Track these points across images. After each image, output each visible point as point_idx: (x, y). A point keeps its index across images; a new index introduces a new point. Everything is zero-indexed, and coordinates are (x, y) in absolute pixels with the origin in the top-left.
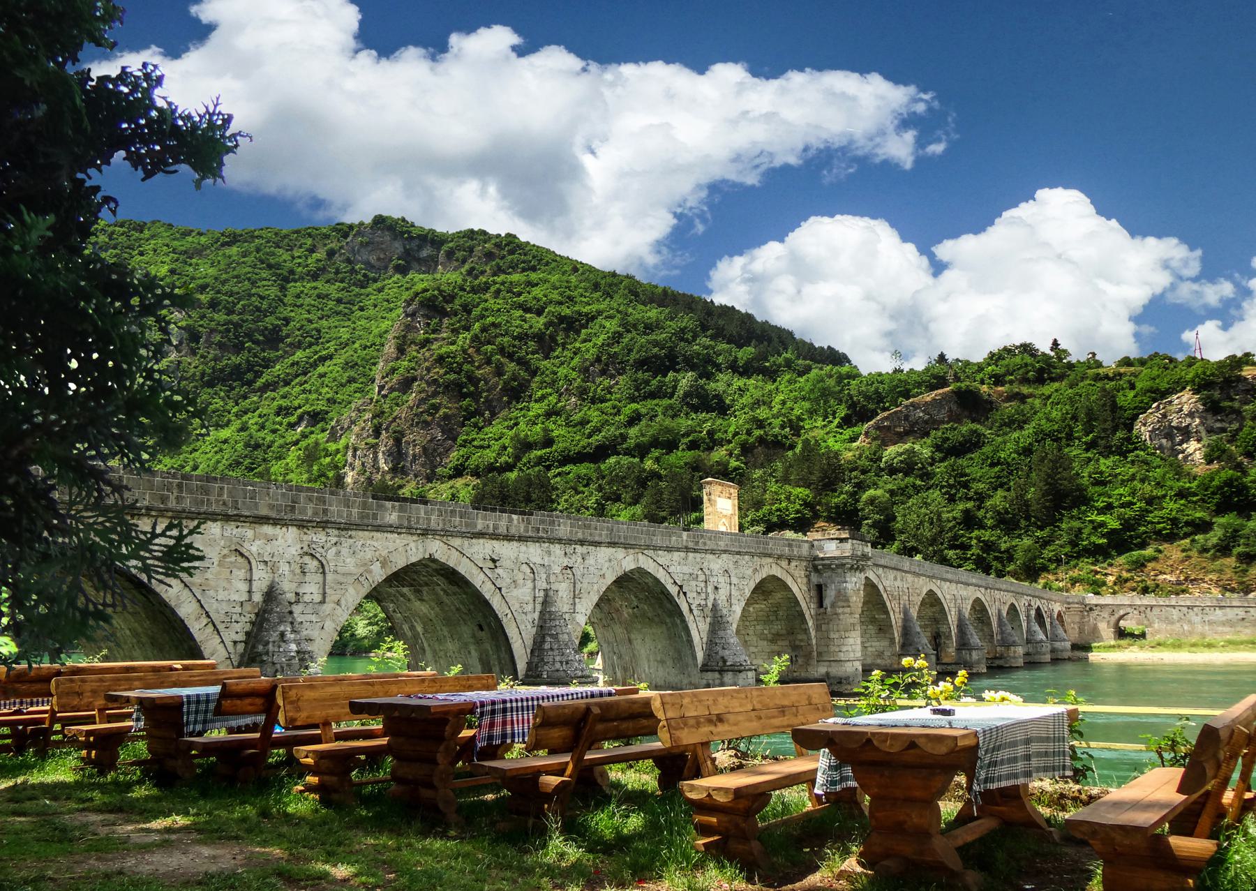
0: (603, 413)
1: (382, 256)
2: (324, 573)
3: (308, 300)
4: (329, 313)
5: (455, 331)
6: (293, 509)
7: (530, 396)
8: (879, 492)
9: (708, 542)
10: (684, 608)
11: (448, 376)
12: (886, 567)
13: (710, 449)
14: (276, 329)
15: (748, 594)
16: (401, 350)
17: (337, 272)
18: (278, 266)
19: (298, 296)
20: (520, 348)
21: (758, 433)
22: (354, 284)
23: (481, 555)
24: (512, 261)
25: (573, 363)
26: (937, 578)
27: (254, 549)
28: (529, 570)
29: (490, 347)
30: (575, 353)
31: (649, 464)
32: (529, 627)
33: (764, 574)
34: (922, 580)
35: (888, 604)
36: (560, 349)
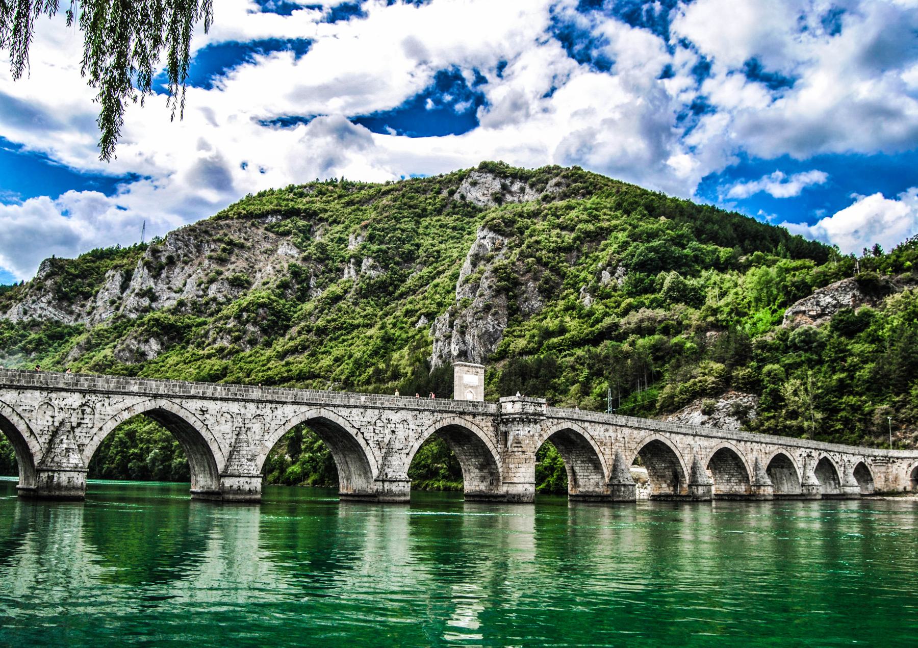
0: (607, 306)
1: (486, 192)
3: (433, 230)
5: (511, 248)
7: (558, 296)
8: (776, 366)
11: (499, 284)
13: (678, 333)
14: (410, 251)
16: (474, 265)
17: (455, 207)
18: (415, 207)
19: (427, 228)
20: (554, 259)
21: (711, 319)
22: (466, 215)
25: (591, 268)
26: (664, 431)
27: (56, 402)
28: (229, 416)
29: (530, 260)
30: (594, 260)
31: (625, 346)
32: (227, 446)
34: (642, 433)
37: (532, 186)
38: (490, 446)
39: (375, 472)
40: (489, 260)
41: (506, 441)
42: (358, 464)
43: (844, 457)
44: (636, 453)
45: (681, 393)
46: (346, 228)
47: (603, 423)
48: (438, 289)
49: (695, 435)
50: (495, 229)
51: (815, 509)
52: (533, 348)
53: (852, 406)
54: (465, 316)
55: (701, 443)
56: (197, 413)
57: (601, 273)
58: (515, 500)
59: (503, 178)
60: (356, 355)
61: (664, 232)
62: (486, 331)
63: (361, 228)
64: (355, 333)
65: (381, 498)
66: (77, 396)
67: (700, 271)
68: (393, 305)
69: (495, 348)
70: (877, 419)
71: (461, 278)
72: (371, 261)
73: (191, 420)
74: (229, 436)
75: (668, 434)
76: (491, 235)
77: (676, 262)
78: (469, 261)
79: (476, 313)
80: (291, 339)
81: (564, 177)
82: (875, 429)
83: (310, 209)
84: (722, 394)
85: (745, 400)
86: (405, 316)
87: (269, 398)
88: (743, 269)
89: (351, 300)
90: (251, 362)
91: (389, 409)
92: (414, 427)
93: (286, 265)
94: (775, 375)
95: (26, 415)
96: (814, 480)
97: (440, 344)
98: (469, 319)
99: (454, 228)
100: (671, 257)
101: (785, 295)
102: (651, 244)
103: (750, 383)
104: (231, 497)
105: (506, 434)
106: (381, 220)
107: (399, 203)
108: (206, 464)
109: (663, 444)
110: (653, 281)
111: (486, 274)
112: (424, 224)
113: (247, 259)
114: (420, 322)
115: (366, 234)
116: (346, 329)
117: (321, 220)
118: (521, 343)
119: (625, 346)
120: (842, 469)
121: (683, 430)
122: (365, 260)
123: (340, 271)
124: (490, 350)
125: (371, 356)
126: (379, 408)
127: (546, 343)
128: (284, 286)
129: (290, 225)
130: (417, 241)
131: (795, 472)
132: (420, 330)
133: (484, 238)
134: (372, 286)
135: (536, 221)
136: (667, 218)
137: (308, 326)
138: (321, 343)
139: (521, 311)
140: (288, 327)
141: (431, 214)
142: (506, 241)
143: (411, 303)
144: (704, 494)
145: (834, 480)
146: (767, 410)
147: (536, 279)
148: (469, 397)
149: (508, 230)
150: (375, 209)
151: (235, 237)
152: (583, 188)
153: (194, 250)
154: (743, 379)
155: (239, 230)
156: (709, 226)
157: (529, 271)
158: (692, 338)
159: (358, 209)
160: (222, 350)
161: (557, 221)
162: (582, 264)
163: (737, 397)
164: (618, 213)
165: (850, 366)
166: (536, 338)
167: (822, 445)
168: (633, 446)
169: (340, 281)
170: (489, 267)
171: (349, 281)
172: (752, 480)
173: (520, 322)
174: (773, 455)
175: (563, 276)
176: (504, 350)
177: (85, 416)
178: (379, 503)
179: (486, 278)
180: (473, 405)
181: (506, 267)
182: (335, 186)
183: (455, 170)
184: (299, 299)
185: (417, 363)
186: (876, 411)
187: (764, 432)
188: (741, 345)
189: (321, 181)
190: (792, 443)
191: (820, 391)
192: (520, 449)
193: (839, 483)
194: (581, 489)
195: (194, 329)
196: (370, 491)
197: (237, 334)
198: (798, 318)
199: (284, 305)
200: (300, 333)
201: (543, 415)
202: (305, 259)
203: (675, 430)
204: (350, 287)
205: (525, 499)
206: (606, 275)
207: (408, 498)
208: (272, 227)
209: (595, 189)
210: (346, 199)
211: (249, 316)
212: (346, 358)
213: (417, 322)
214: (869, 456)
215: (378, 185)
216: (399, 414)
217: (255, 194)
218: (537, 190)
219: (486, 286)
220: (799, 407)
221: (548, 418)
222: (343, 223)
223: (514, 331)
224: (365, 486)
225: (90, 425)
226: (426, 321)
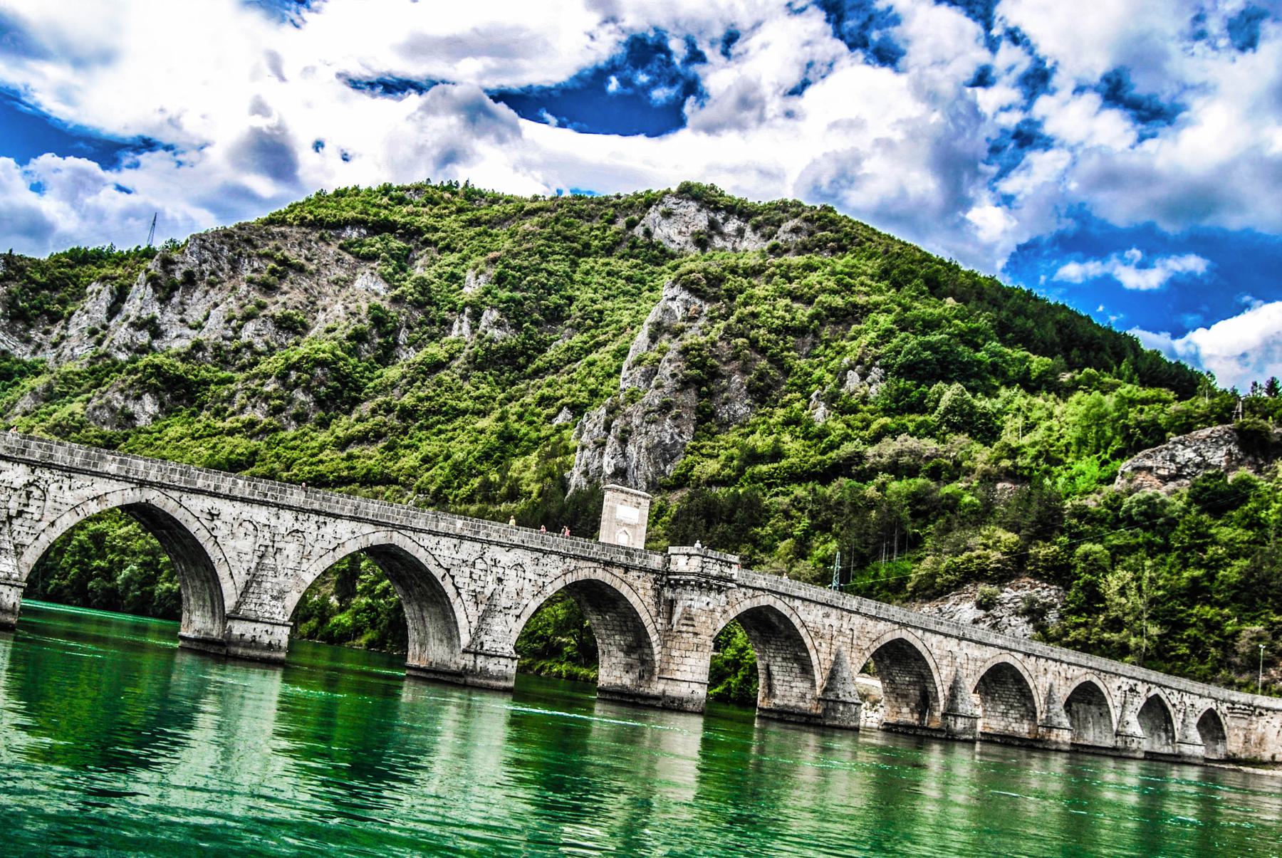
0: (849, 426)
1: (684, 229)
3: (597, 278)
4: (615, 293)
5: (712, 320)
6: (23, 452)
7: (777, 401)
8: (1098, 547)
10: (450, 590)
12: (810, 601)
16: (653, 338)
17: (634, 246)
18: (573, 239)
19: (587, 273)
20: (777, 343)
21: (1006, 463)
22: (649, 261)
24: (819, 240)
26: (915, 627)
29: (740, 341)
30: (838, 353)
31: (870, 490)
32: (243, 573)
34: (881, 625)
36: (822, 347)
37: (756, 228)
38: (645, 617)
39: (465, 639)
40: (677, 333)
41: (671, 614)
42: (441, 623)
43: (1186, 699)
44: (868, 655)
45: (947, 572)
46: (464, 259)
47: (823, 604)
48: (594, 369)
49: (961, 639)
50: (691, 287)
51: (1133, 774)
52: (729, 476)
53: (1206, 621)
54: (631, 416)
55: (969, 651)
56: (203, 517)
57: (845, 374)
58: (675, 706)
59: (712, 210)
60: (455, 456)
61: (949, 321)
62: (660, 442)
63: (487, 263)
64: (459, 422)
65: (470, 679)
67: (997, 388)
68: (522, 386)
69: (670, 470)
70: (1243, 646)
71: (631, 357)
73: (193, 526)
74: (248, 557)
75: (920, 632)
76: (685, 295)
77: (963, 370)
79: (648, 413)
80: (360, 420)
81: (806, 220)
82: (1237, 660)
83: (411, 224)
84: (1010, 579)
85: (1045, 593)
86: (539, 404)
87: (316, 506)
88: (1064, 392)
89: (459, 371)
90: (294, 448)
91: (498, 544)
92: (533, 577)
93: (365, 306)
94: (1095, 560)
96: (1135, 728)
97: (587, 453)
98: (636, 421)
99: (629, 279)
100: (956, 361)
101: (1124, 439)
102: (927, 338)
103: (1054, 568)
104: (240, 651)
105: (671, 604)
106: (518, 253)
107: (548, 230)
108: (207, 597)
109: (911, 646)
110: (924, 395)
111: (670, 355)
112: (584, 267)
113: (306, 290)
114: (561, 416)
115: (492, 272)
116: (446, 413)
117: (427, 243)
118: (712, 467)
119: (870, 490)
120: (1181, 716)
121: (943, 629)
122: (487, 313)
123: (447, 324)
124: (663, 472)
125: (479, 460)
126: (482, 541)
127: (749, 470)
128: (359, 337)
129: (378, 245)
130: (570, 292)
131: (1109, 712)
132: (559, 430)
133: (673, 299)
134: (494, 353)
135: (755, 282)
136: (958, 301)
137: (388, 404)
138: (405, 432)
139: (717, 417)
140: (356, 402)
141: (596, 253)
142: (706, 308)
143: (549, 385)
144: (964, 731)
145: (1166, 731)
146: (1077, 612)
147: (745, 371)
148: (623, 540)
149: (711, 291)
150: (511, 236)
151: (292, 254)
152: (833, 241)
153: (227, 267)
154: (1045, 560)
155: (300, 244)
156: (1019, 321)
157: (736, 357)
158: (975, 489)
159: (485, 233)
160: (252, 424)
161: (787, 286)
162: (818, 356)
163: (1032, 588)
164: (883, 285)
165: (1211, 559)
166: (735, 462)
167: (1155, 676)
168: (865, 644)
169: (444, 339)
170: (676, 345)
171: (458, 341)
172: (1041, 717)
173: (713, 434)
174: (1077, 683)
175: (788, 372)
176: (683, 475)
178: (465, 686)
179: (670, 361)
180: (628, 554)
181: (701, 347)
182: (454, 194)
183: (641, 190)
184: (378, 360)
185: (549, 479)
186: (1243, 634)
187: (1067, 645)
188: (1048, 508)
189: (433, 184)
190: (1108, 668)
191: (1161, 593)
192: (691, 629)
193: (1173, 737)
194: (777, 701)
195: (213, 387)
196: (453, 667)
197: (278, 402)
198: (1140, 478)
199: (355, 367)
200: (374, 412)
201: (732, 581)
202: (396, 300)
203: (932, 627)
204: (460, 351)
205: (690, 707)
206: (853, 378)
207: (511, 684)
208: (351, 245)
209: (852, 243)
210: (470, 215)
211: (299, 378)
212: (441, 458)
213: (556, 415)
214: (1224, 701)
215: (521, 200)
216: (511, 554)
217: (330, 192)
218: (763, 236)
219: (667, 372)
220: (1125, 614)
221: (739, 586)
222: (460, 251)
223: (703, 447)
224: (447, 658)
226: (570, 416)
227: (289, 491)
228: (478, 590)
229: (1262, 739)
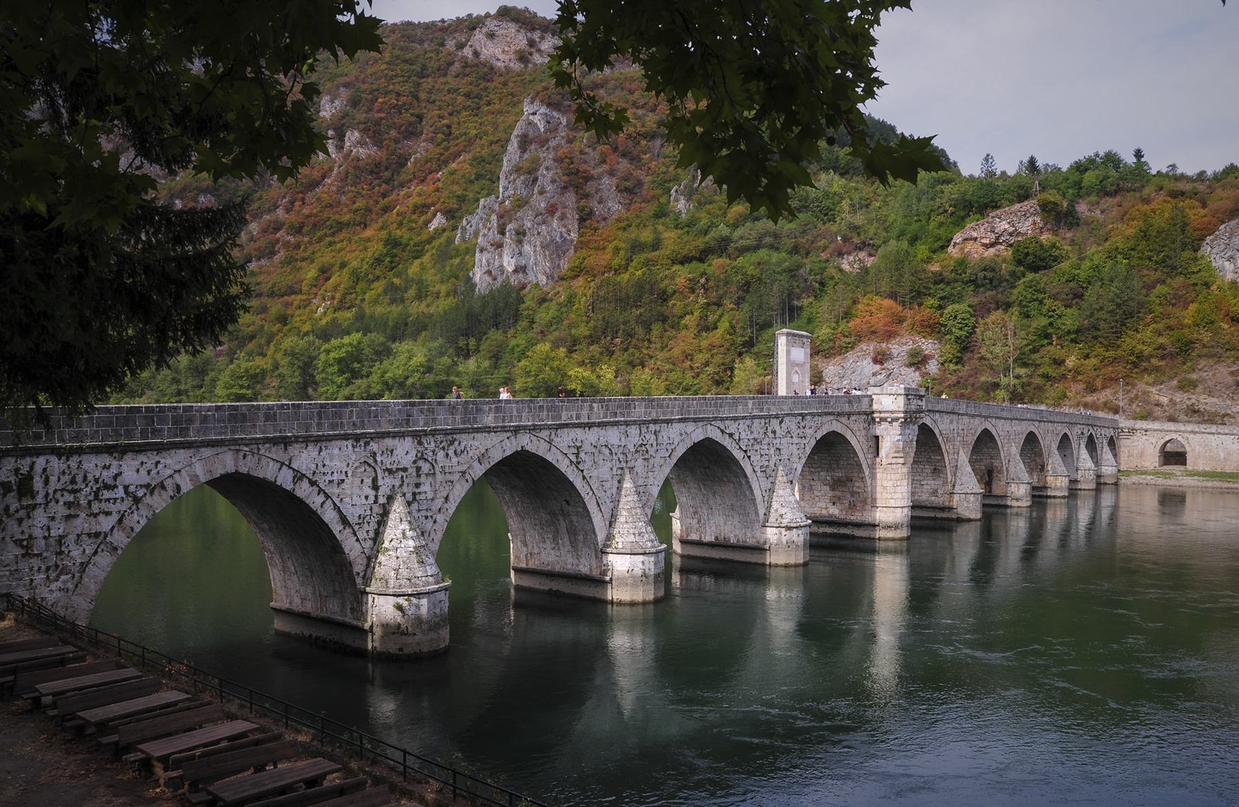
1: (506, 49)
2: (434, 474)
9: (772, 408)
10: (748, 471)
14: (411, 124)
15: (808, 451)
19: (430, 92)
23: (566, 443)
28: (607, 451)
32: (608, 502)
33: (824, 431)
35: (943, 446)
40: (543, 142)
66: (408, 443)
72: (356, 134)
73: (564, 466)
76: (543, 110)
78: (516, 145)
87: (654, 416)
91: (776, 417)
95: (333, 490)
99: (467, 95)
122: (348, 134)
130: (416, 112)
133: (534, 114)
147: (611, 173)
157: (604, 161)
166: (622, 253)
177: (423, 479)
200: (264, 231)
216: (783, 425)
225: (430, 495)
226: (444, 221)
227: (632, 406)
228: (766, 463)
229: (1142, 453)
